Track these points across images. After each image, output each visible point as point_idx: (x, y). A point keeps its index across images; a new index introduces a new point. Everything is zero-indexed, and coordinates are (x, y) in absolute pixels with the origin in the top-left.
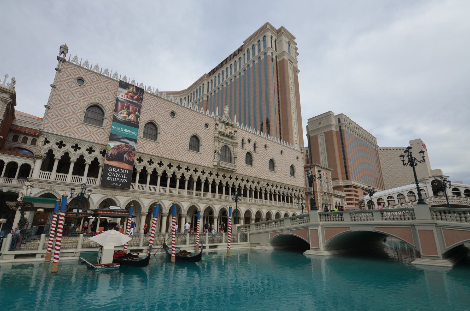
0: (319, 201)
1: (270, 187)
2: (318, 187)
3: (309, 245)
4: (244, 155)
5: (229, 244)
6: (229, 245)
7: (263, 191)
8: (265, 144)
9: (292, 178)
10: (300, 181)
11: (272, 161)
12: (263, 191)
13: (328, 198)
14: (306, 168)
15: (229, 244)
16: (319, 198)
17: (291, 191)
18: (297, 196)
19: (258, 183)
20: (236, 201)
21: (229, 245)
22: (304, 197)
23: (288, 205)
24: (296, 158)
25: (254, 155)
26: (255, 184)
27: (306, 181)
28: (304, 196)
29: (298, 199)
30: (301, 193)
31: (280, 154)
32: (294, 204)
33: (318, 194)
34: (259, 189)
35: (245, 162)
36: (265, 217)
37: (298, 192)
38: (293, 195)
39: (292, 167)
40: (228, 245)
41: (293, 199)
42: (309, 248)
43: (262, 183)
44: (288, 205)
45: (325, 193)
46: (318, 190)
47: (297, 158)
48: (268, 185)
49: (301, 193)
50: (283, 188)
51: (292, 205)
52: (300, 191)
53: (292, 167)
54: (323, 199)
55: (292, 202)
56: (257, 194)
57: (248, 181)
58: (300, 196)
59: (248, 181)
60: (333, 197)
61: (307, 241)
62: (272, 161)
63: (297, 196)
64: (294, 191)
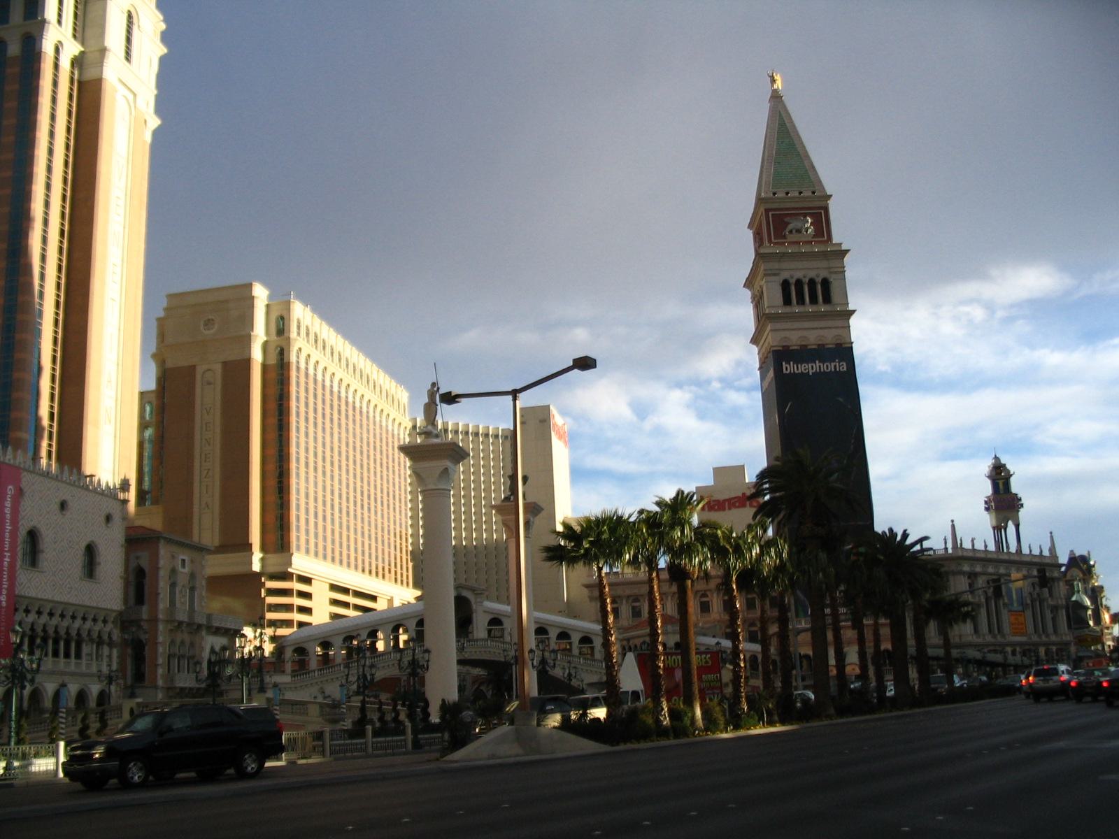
0: (161, 650)
2: (161, 606)
13: (187, 638)
16: (161, 639)
28: (116, 635)
29: (100, 643)
30: (110, 626)
33: (161, 627)
38: (84, 635)
39: (90, 551)
41: (84, 646)
45: (180, 623)
46: (161, 616)
47: (108, 518)
49: (110, 626)
50: (68, 617)
53: (90, 551)
54: (173, 642)
55: (78, 656)
58: (105, 637)
60: (204, 633)
63: (95, 635)
64: (89, 624)
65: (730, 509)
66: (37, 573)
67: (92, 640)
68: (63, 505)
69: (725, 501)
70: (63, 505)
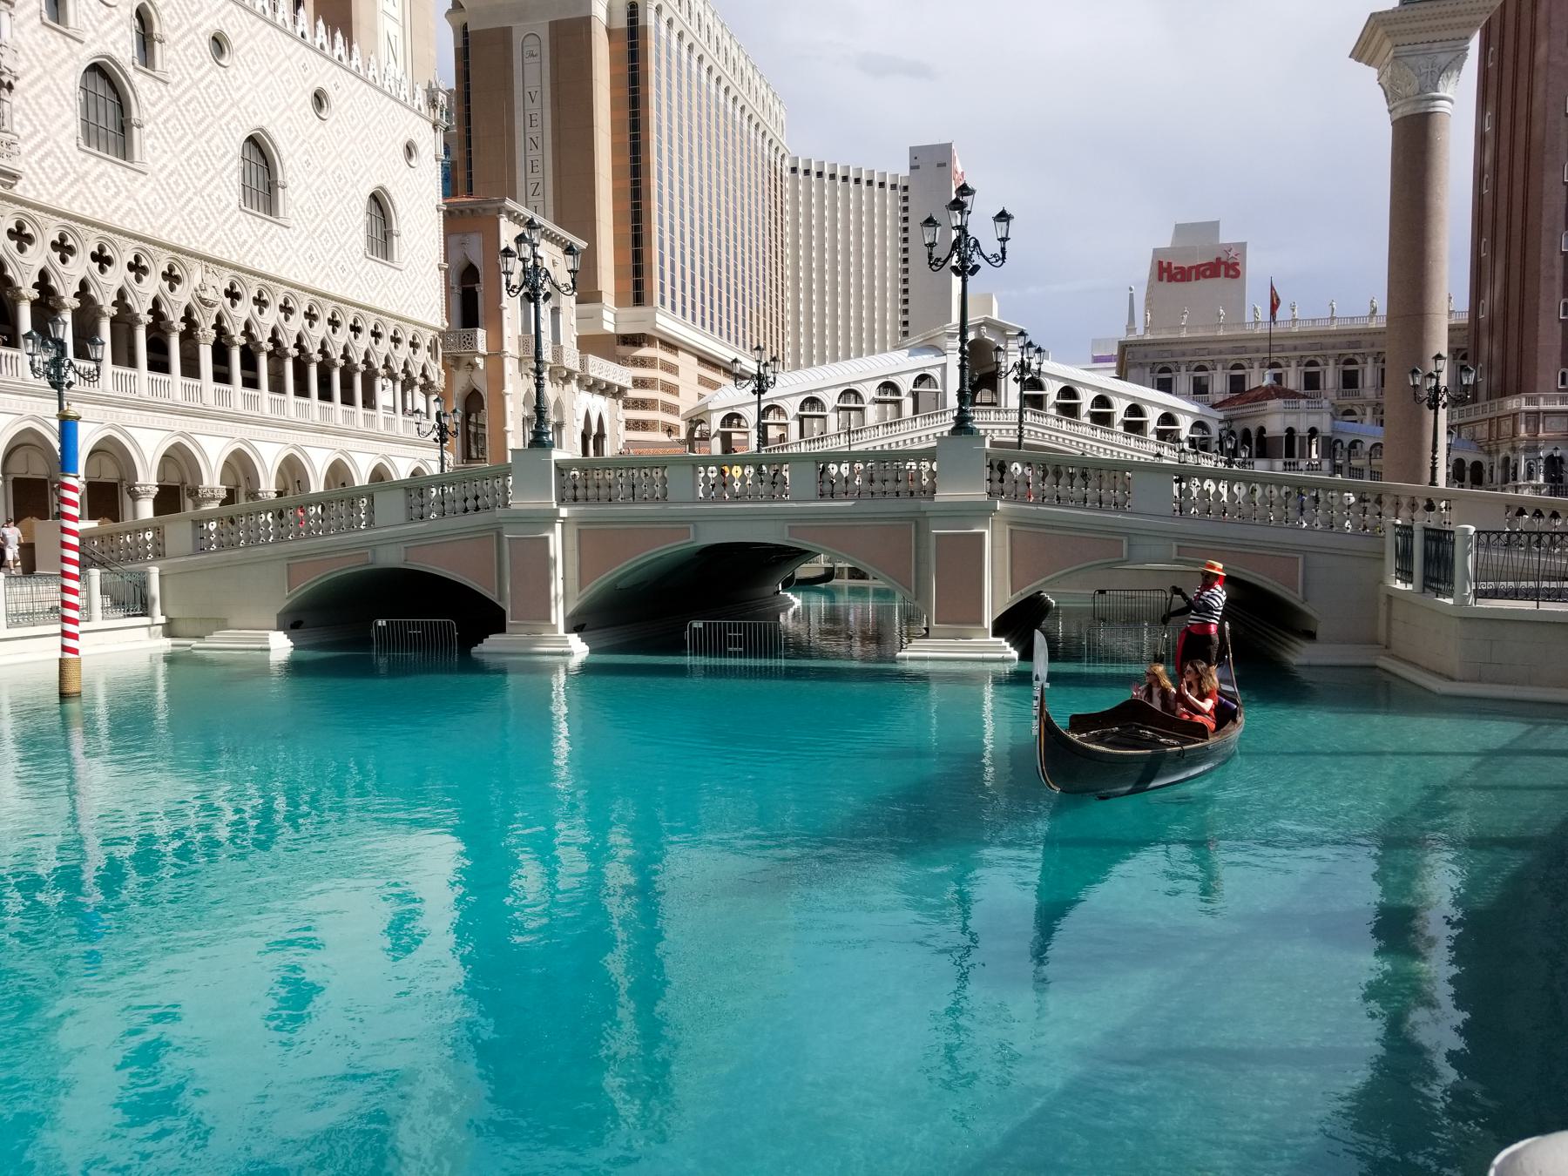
1: (244, 310)
3: (503, 612)
4: (70, 79)
5: (70, 628)
6: (75, 637)
7: (207, 335)
8: (211, 25)
9: (376, 267)
10: (415, 290)
11: (258, 147)
12: (207, 335)
14: (455, 221)
15: (70, 628)
17: (365, 340)
18: (398, 369)
19: (171, 277)
20: (57, 384)
21: (75, 637)
22: (433, 377)
23: (349, 417)
24: (401, 150)
25: (141, 86)
26: (153, 285)
27: (448, 289)
28: (437, 374)
29: (408, 384)
30: (423, 355)
31: (309, 108)
32: (380, 413)
34: (175, 317)
35: (75, 127)
36: (216, 483)
37: (404, 351)
38: (379, 365)
39: (379, 203)
40: (65, 634)
41: (379, 383)
42: (500, 628)
43: (195, 276)
44: (349, 417)
47: (410, 150)
48: (233, 295)
51: (369, 421)
52: (414, 345)
53: (379, 203)
55: (369, 402)
56: (159, 343)
57: (102, 259)
58: (416, 373)
59: (102, 259)
60: (574, 383)
61: (493, 597)
62: (258, 147)
64: (385, 345)
65: (1197, 278)
66: (276, 227)
67: (392, 377)
68: (319, 99)
69: (1191, 268)
70: (319, 99)
